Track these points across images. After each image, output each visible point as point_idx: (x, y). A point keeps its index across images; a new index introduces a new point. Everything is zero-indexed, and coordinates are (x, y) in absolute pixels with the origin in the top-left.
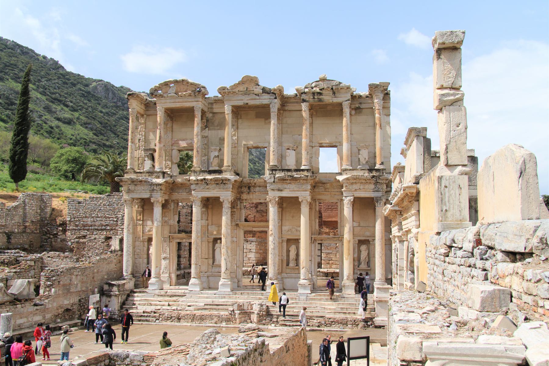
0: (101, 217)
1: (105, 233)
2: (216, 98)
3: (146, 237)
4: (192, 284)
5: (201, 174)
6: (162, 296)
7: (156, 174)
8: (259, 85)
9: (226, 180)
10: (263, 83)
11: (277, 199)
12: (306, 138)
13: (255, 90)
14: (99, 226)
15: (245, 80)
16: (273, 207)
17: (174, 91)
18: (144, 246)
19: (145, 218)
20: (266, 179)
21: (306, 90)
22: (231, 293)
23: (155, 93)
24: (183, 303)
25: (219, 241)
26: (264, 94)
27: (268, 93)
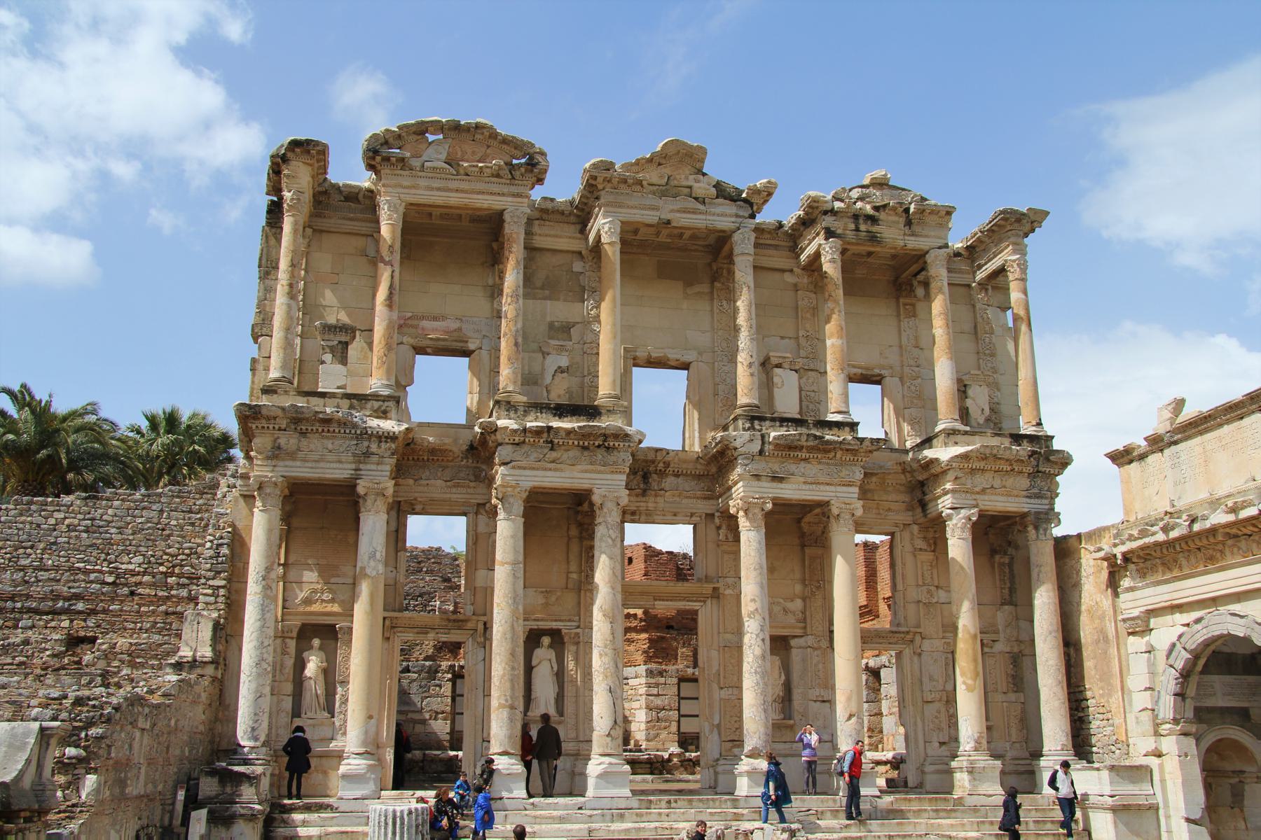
0: (56, 568)
1: (66, 624)
2: (549, 205)
3: (296, 622)
5: (532, 416)
7: (376, 404)
8: (704, 174)
10: (716, 169)
11: (769, 506)
12: (840, 337)
13: (696, 185)
14: (43, 599)
15: (672, 151)
16: (757, 528)
17: (443, 156)
18: (284, 653)
19: (292, 559)
20: (738, 444)
21: (838, 205)
22: (634, 802)
23: (385, 151)
25: (546, 640)
26: (720, 200)
27: (733, 200)
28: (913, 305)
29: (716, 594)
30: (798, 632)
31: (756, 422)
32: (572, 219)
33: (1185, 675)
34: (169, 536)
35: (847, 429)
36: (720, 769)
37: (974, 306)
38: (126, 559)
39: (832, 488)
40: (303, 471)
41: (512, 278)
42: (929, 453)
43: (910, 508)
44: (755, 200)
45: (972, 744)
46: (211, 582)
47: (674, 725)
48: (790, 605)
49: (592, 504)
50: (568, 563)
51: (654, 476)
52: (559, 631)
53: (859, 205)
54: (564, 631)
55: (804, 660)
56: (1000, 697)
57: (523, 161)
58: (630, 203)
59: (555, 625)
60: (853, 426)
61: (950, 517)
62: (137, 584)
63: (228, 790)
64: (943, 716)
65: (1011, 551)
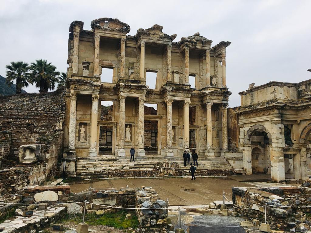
1: (27, 121)
2: (130, 37)
4: (120, 152)
6: (100, 160)
7: (95, 79)
8: (162, 32)
9: (143, 87)
10: (164, 31)
11: (173, 101)
15: (156, 27)
17: (108, 26)
19: (78, 109)
20: (167, 89)
21: (189, 40)
24: (119, 165)
25: (128, 126)
28: (202, 60)
29: (161, 118)
30: (177, 125)
31: (171, 85)
32: (134, 40)
33: (250, 136)
34: (48, 103)
35: (188, 86)
36: (161, 151)
37: (214, 61)
38: (39, 108)
39: (185, 98)
40: (81, 92)
41: (123, 53)
42: (204, 91)
43: (200, 102)
44: (172, 38)
45: (209, 147)
46: (61, 114)
47: (150, 141)
48: (176, 120)
49: (138, 100)
50: (133, 111)
51: (150, 94)
52: (131, 124)
53: (193, 40)
54: (132, 124)
55: (178, 131)
56: (215, 138)
57: (125, 28)
58: (147, 38)
59: (130, 123)
60: (190, 86)
61: (207, 104)
62: (42, 113)
63: (69, 156)
64: (204, 142)
65: (219, 110)
